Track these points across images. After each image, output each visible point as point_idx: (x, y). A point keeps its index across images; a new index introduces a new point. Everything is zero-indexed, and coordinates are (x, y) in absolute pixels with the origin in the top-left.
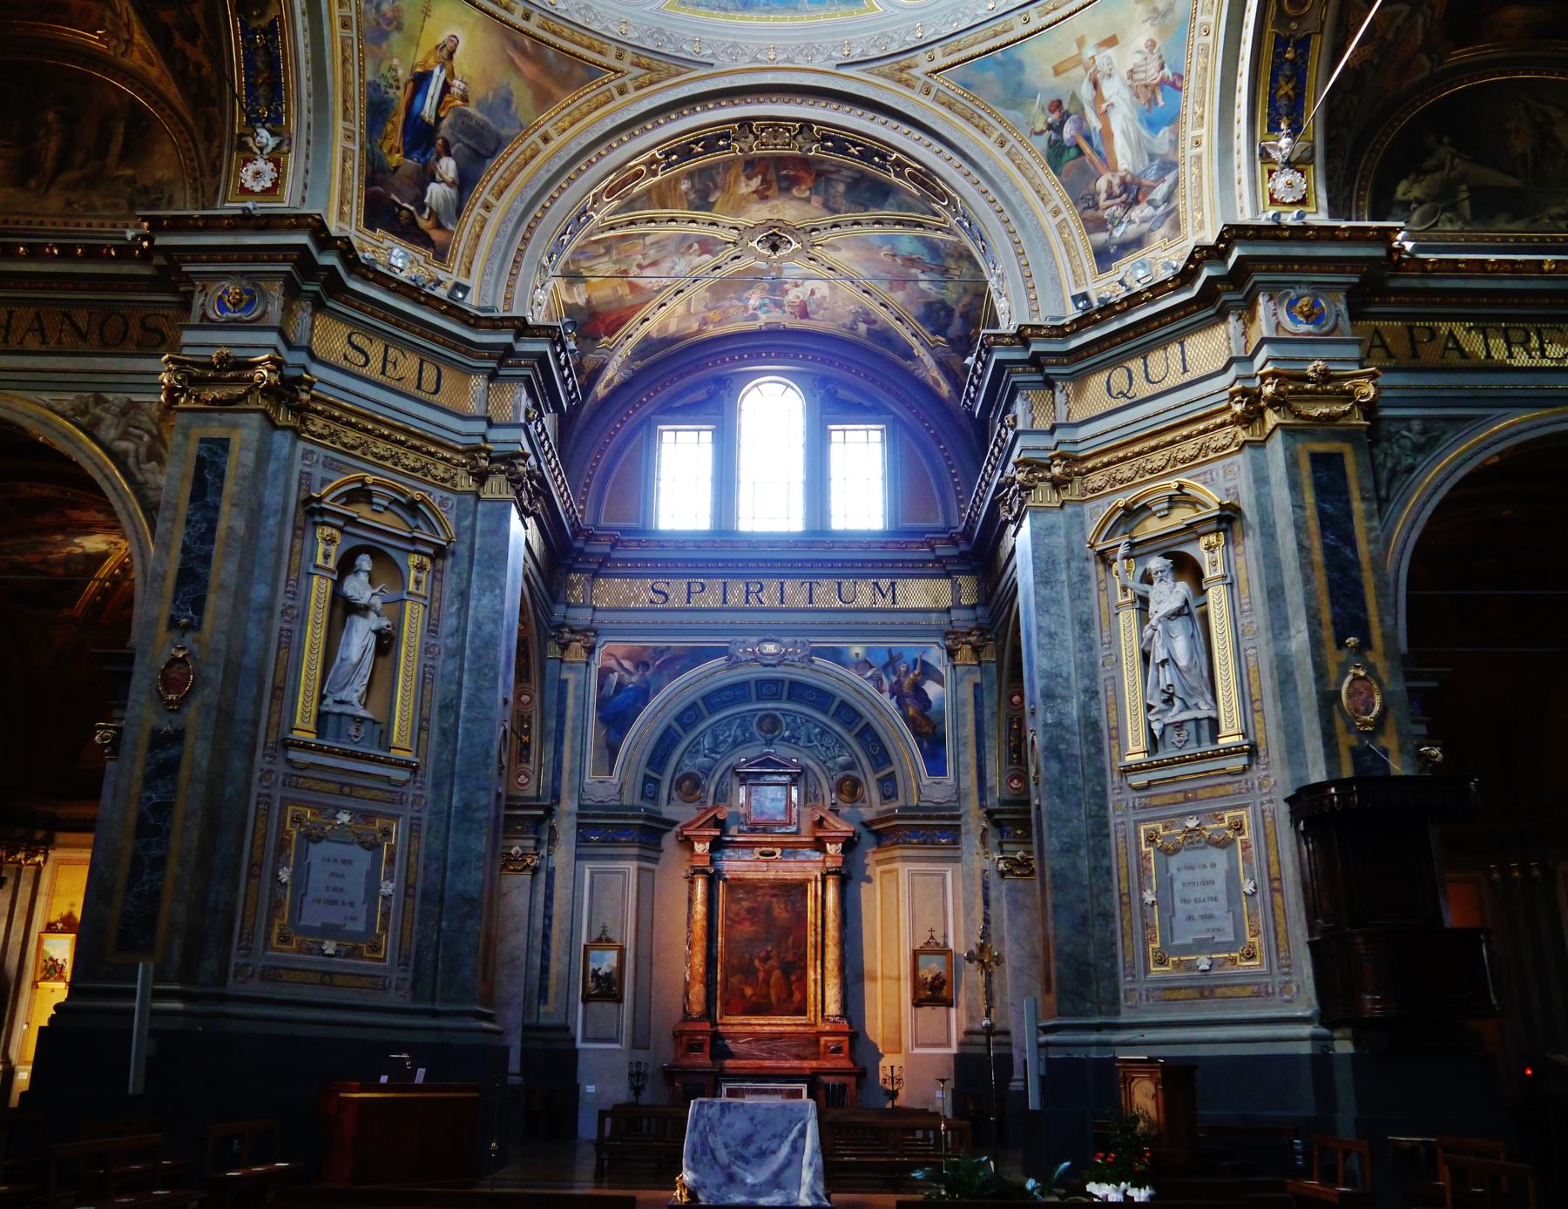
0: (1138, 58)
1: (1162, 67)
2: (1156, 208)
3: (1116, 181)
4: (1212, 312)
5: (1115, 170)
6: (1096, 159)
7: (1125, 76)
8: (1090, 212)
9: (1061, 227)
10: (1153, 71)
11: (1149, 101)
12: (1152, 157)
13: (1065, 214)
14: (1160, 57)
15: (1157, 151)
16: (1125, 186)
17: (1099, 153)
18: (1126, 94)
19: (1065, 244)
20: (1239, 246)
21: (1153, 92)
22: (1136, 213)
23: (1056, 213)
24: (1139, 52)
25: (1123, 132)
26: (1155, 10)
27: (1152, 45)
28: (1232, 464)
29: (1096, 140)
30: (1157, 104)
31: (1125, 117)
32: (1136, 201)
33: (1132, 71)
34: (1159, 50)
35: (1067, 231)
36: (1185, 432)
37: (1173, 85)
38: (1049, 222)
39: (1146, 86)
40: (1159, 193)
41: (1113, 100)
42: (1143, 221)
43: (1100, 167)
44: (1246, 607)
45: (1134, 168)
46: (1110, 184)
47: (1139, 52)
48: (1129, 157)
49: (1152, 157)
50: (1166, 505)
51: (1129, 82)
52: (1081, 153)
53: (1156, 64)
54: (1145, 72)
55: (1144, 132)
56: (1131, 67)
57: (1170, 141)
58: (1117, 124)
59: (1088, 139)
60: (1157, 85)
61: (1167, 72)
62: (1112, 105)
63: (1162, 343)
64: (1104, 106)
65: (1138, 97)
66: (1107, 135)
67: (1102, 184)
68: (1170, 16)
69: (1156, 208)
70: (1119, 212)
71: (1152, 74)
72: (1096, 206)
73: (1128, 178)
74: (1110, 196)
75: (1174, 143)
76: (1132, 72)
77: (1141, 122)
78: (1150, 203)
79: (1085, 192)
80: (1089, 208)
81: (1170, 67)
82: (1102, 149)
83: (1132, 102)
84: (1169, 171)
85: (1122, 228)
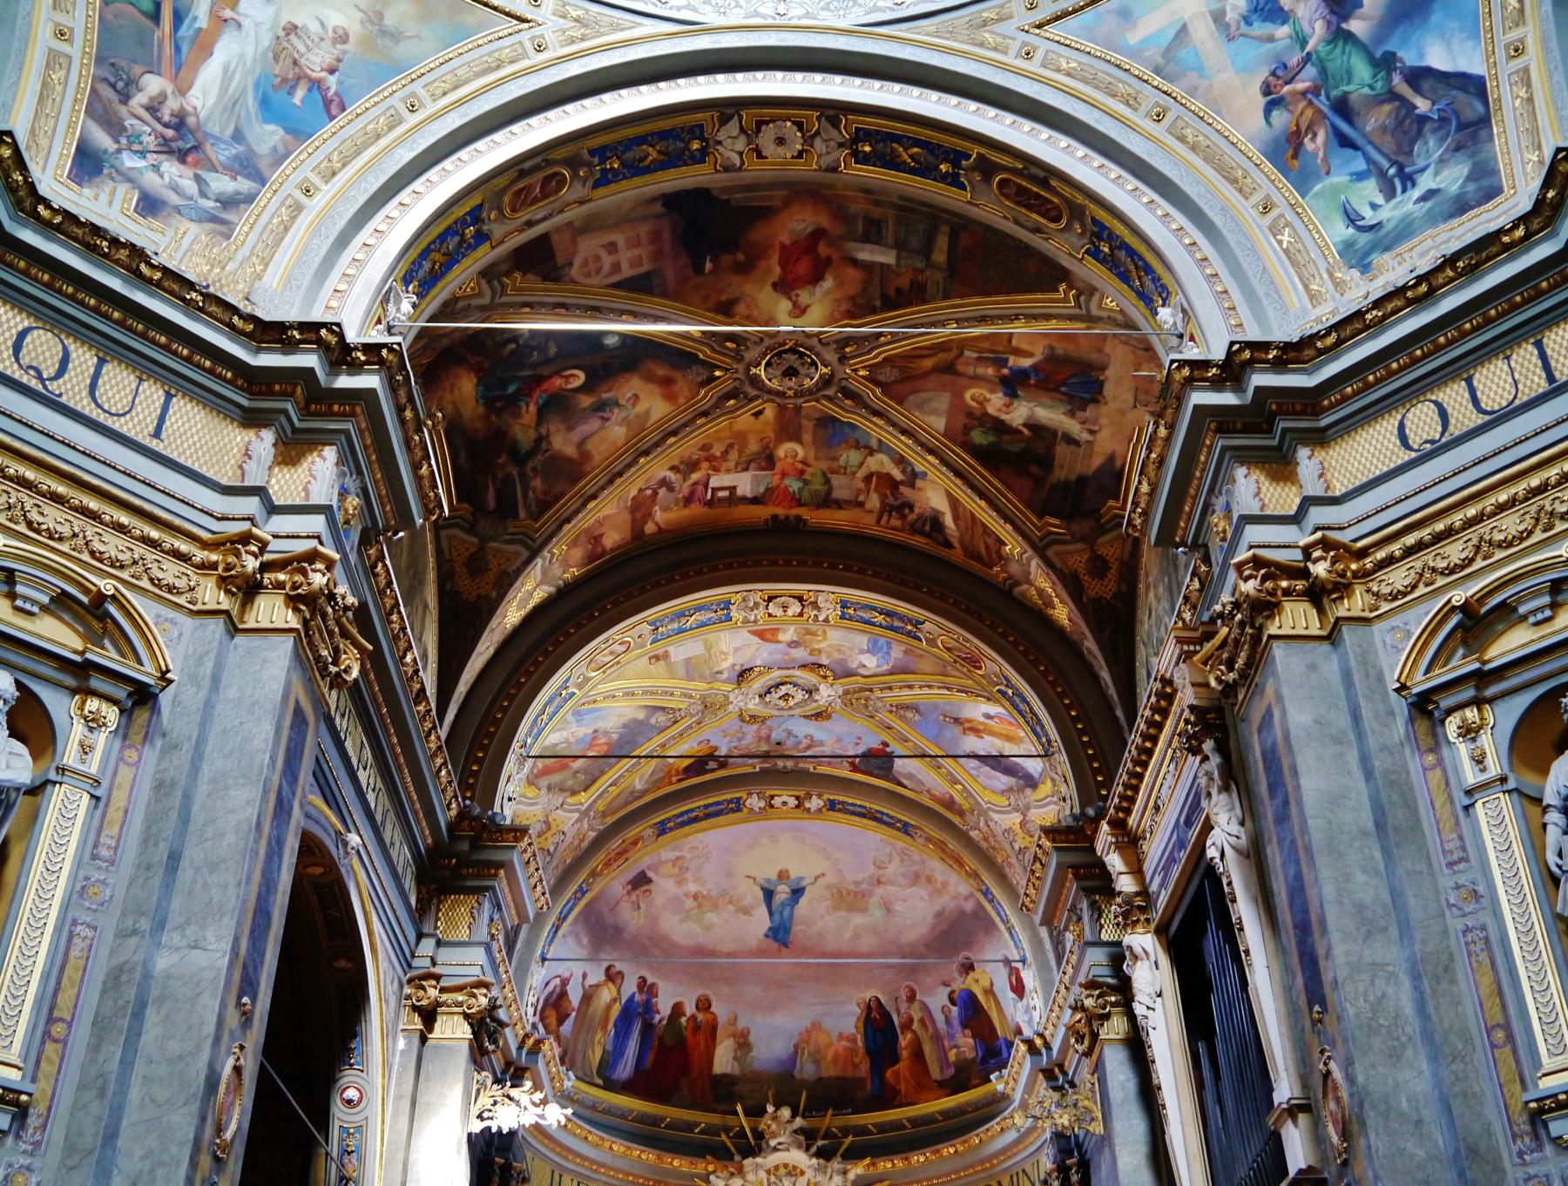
0: (314, 27)
1: (332, 71)
2: (203, 194)
3: (173, 104)
4: (244, 402)
5: (182, 91)
6: (168, 49)
7: (283, 22)
8: (107, 92)
9: (54, 60)
10: (318, 60)
11: (284, 80)
12: (238, 136)
13: (75, 50)
14: (339, 60)
15: (249, 136)
16: (180, 122)
17: (178, 49)
18: (266, 40)
19: (44, 85)
20: (320, 357)
21: (299, 78)
22: (171, 168)
23: (61, 34)
24: (322, 24)
25: (226, 68)
26: (380, 16)
27: (343, 38)
28: (172, 621)
29: (185, 31)
30: (291, 93)
31: (242, 56)
32: (182, 156)
33: (296, 27)
34: (345, 52)
35: (62, 73)
36: (124, 518)
37: (327, 104)
38: (43, 37)
39: (295, 63)
40: (222, 184)
41: (246, 23)
42: (176, 189)
43: (165, 65)
44: (104, 853)
45: (208, 118)
46: (162, 98)
47: (322, 24)
48: (211, 101)
49: (238, 136)
50: (45, 600)
51: (282, 34)
52: (155, 17)
53: (329, 60)
54: (309, 49)
55: (251, 101)
56: (299, 24)
57: (275, 149)
58: (226, 50)
59: (178, 18)
60: (310, 79)
61: (332, 82)
62: (240, 25)
63: (146, 368)
64: (228, 13)
65: (276, 59)
66: (204, 46)
67: (153, 85)
68: (388, 42)
69: (203, 194)
70: (150, 141)
71: (316, 61)
72: (125, 98)
73: (191, 121)
74: (153, 109)
75: (279, 159)
76: (292, 29)
77: (257, 86)
78: (198, 178)
79: (123, 63)
80: (113, 86)
81: (340, 83)
82: (185, 48)
83: (264, 54)
84: (248, 176)
85: (141, 164)
